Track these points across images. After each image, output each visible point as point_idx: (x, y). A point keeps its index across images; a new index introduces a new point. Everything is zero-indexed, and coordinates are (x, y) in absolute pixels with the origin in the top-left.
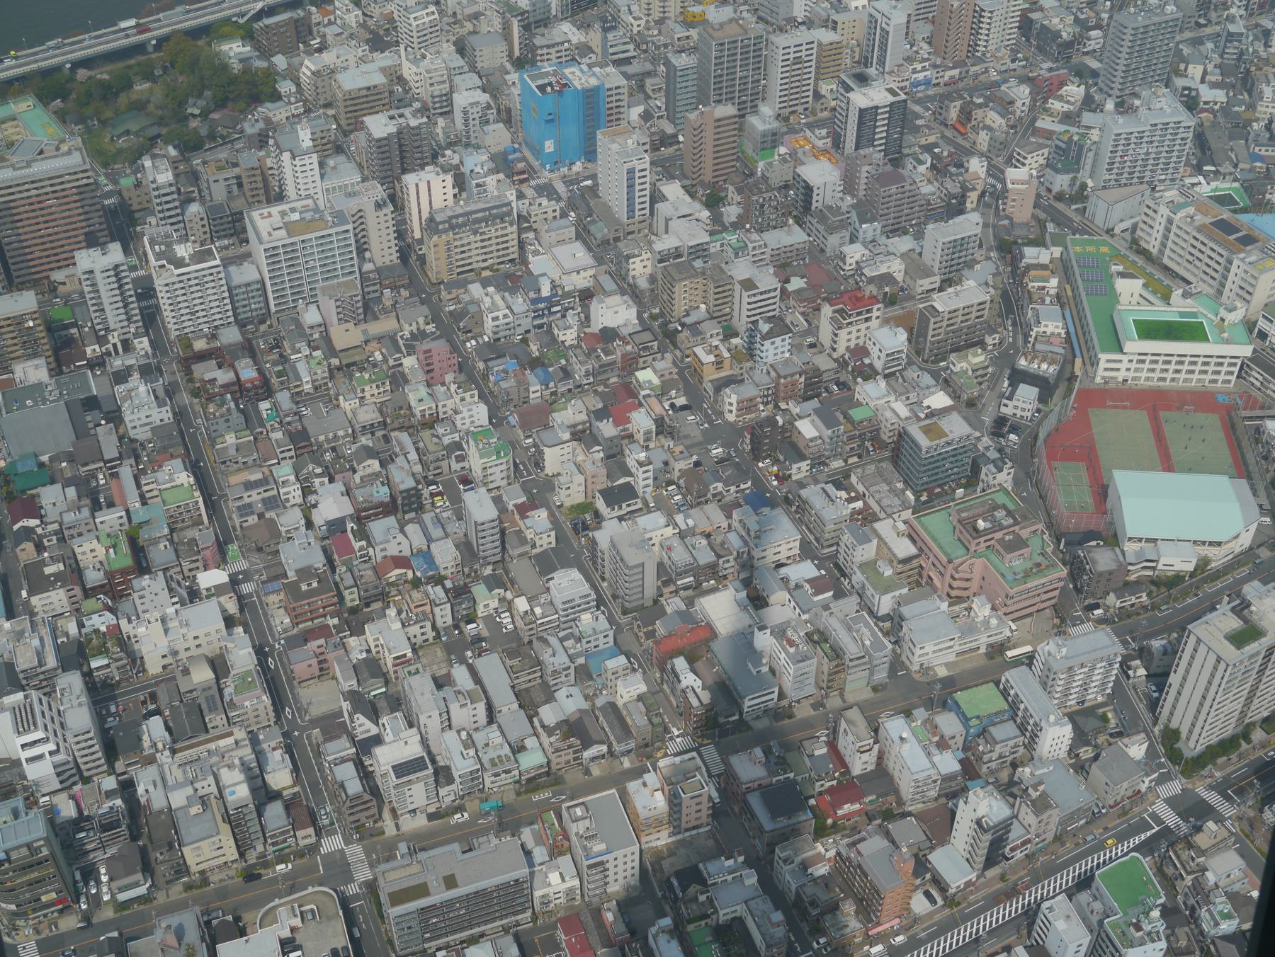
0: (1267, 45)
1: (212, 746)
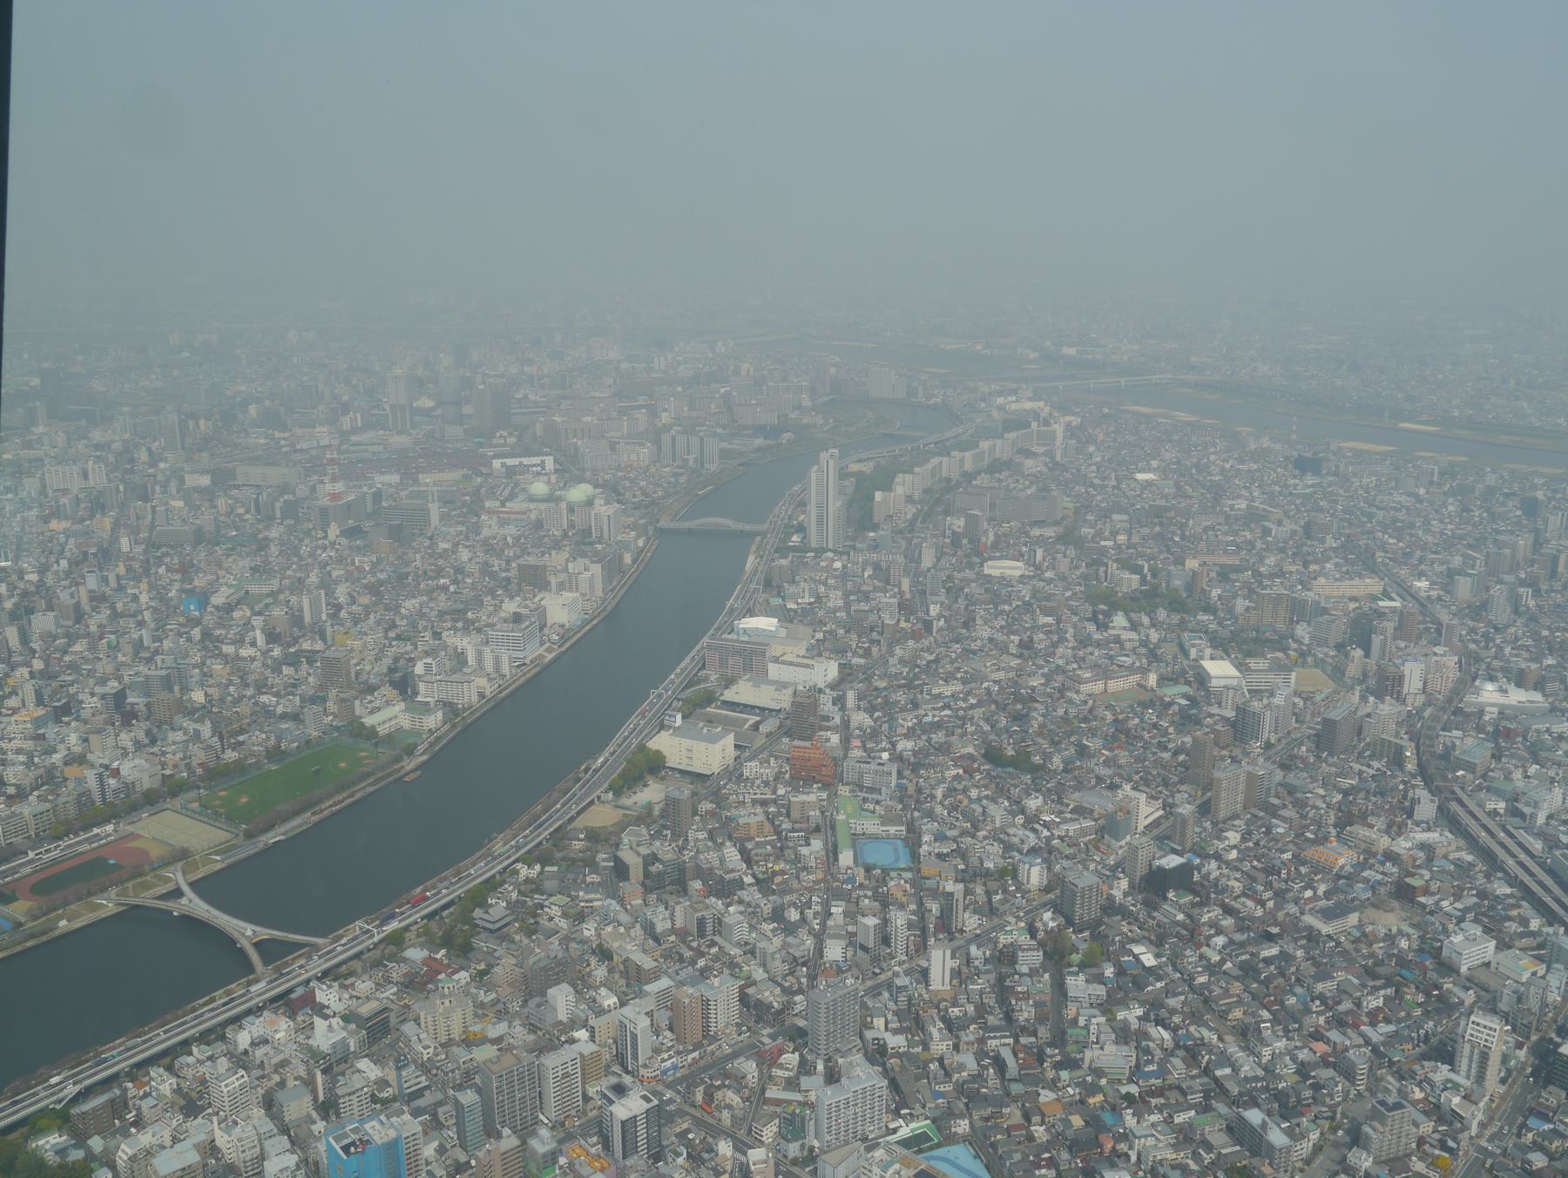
0: (927, 984)
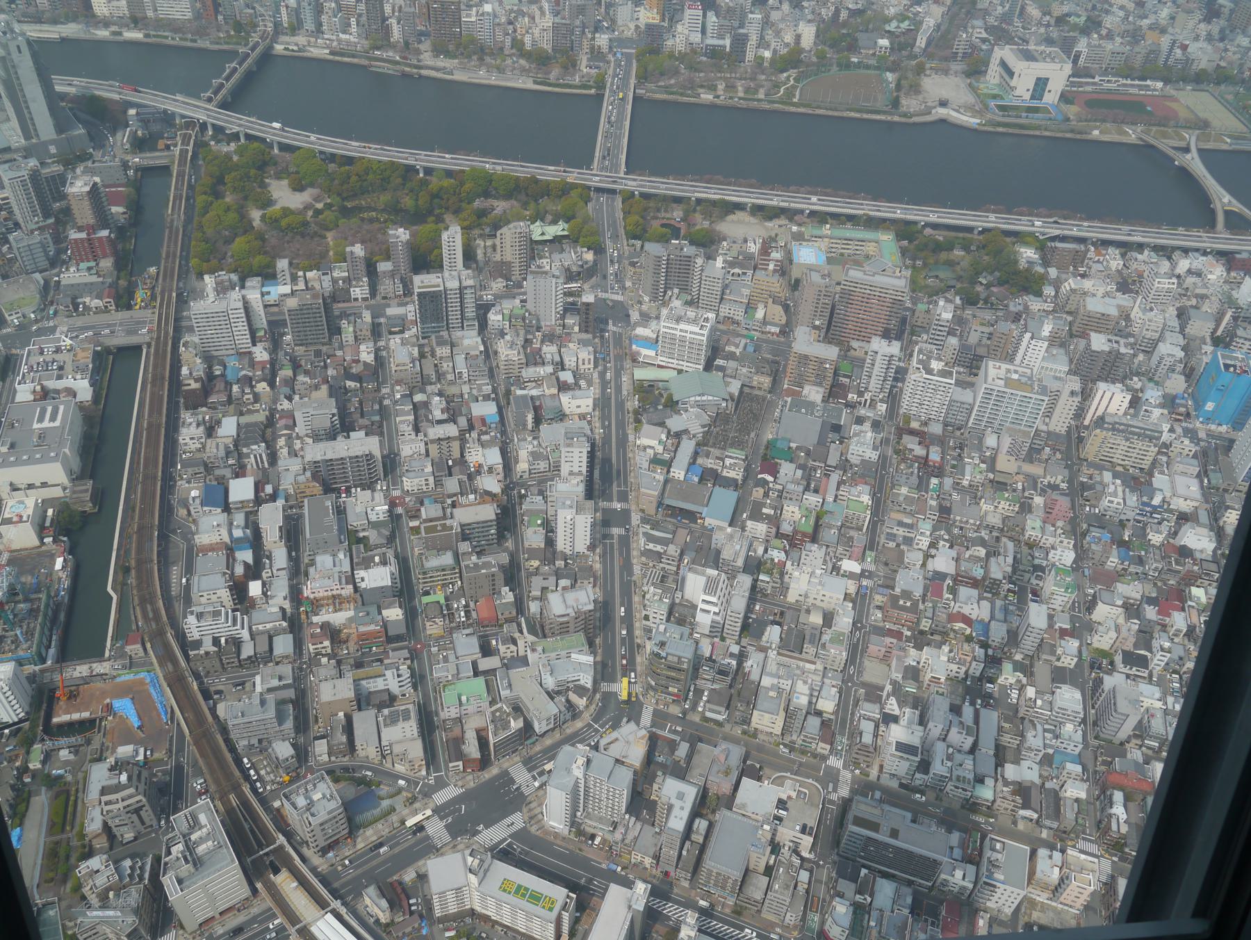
1: (801, 664)
